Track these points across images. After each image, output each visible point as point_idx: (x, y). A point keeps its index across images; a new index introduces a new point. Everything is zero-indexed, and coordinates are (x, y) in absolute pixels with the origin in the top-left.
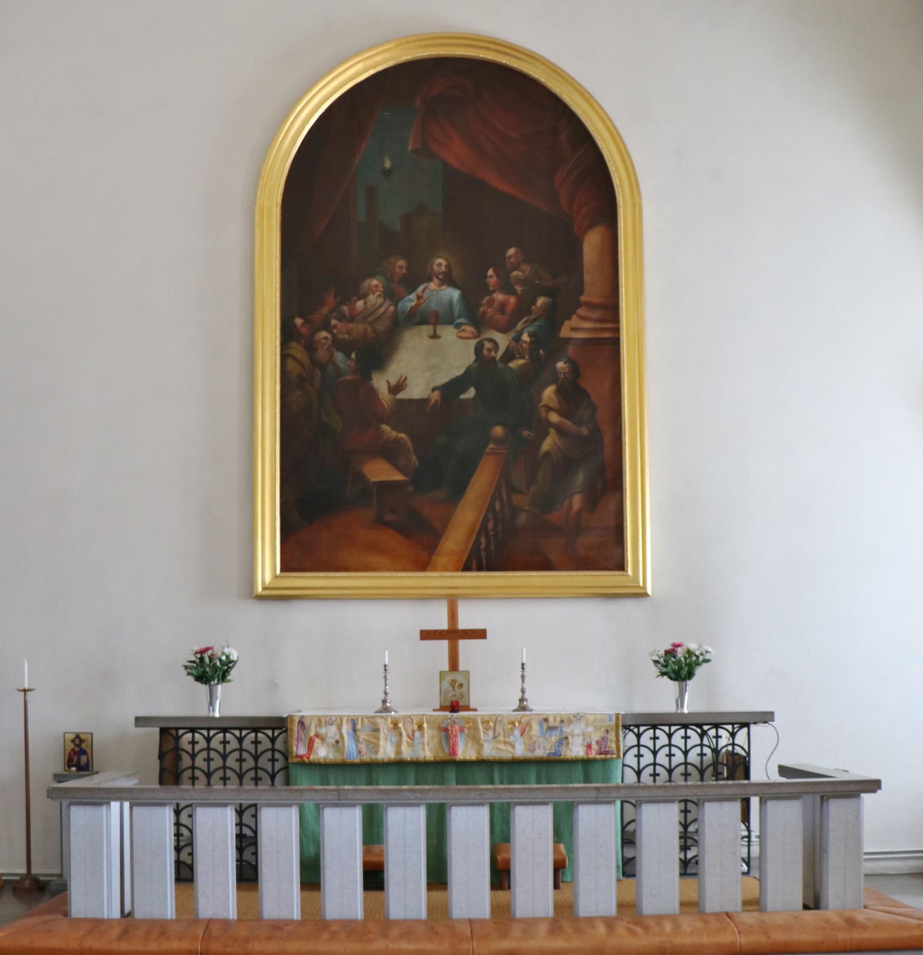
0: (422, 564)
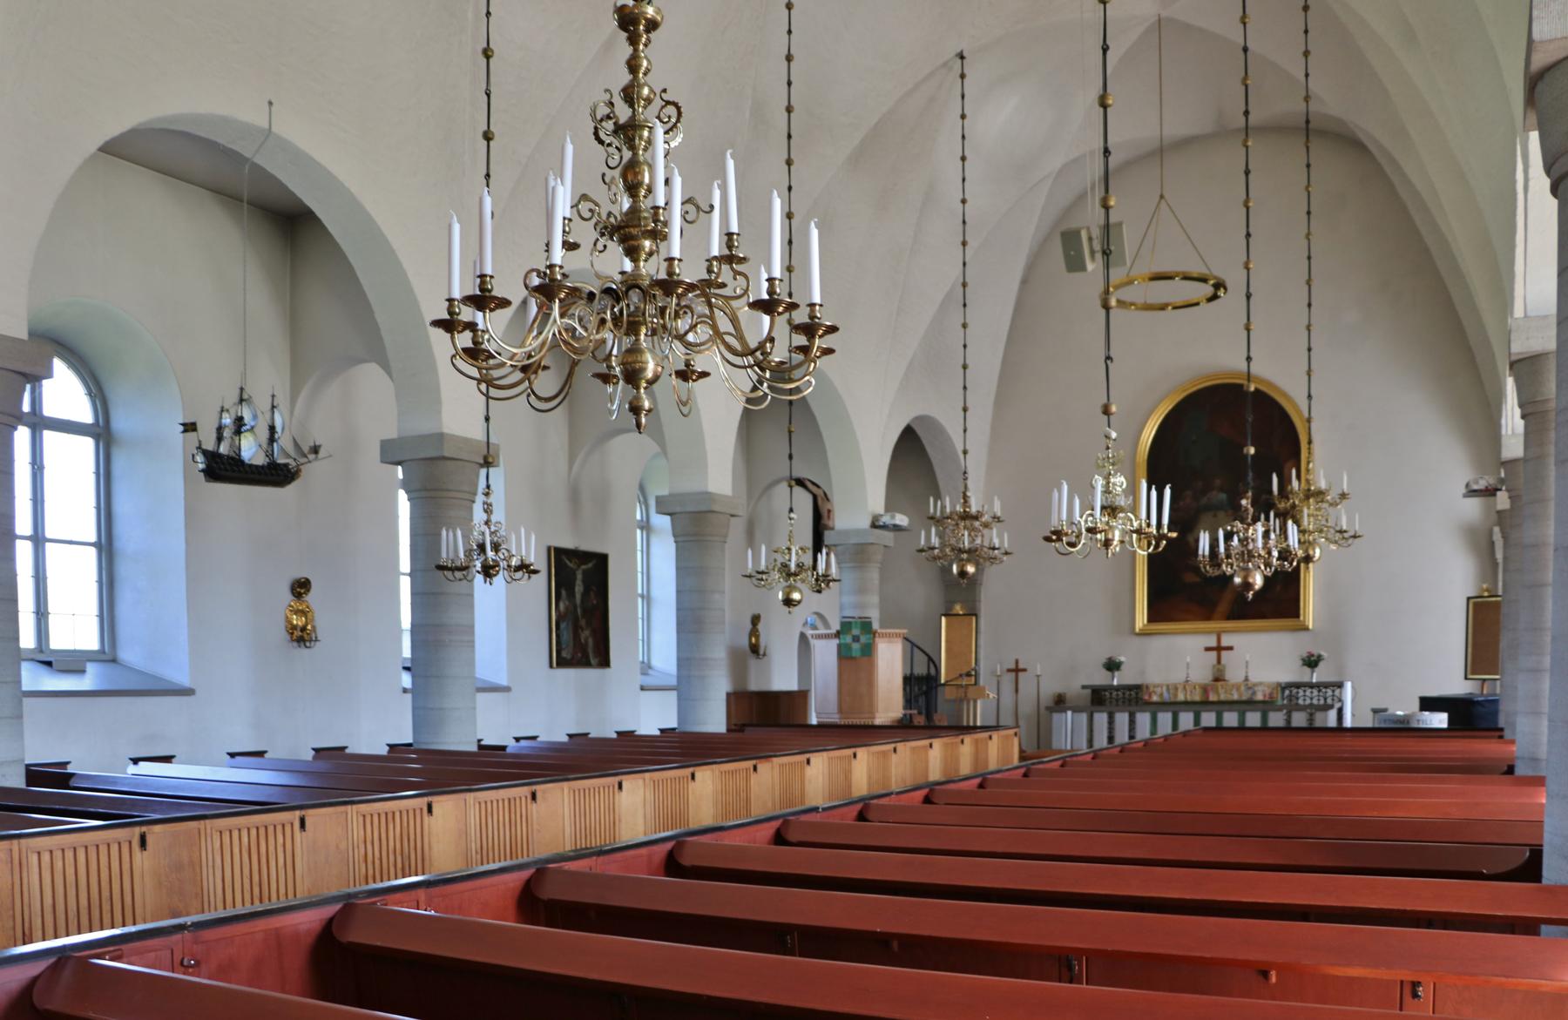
0: (1208, 618)
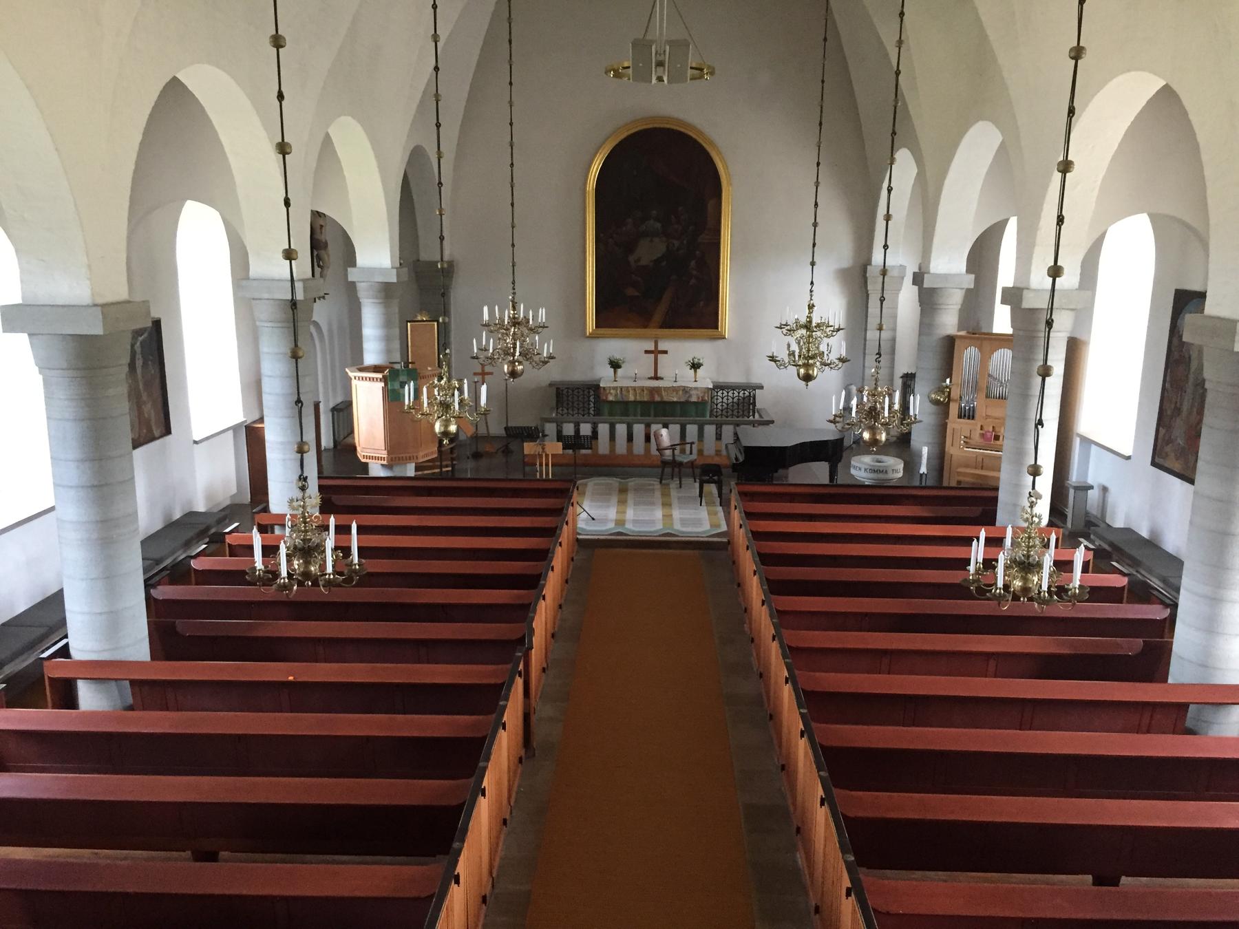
0: (645, 327)
